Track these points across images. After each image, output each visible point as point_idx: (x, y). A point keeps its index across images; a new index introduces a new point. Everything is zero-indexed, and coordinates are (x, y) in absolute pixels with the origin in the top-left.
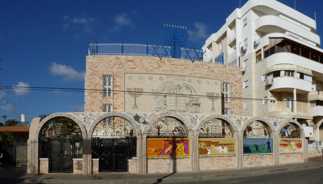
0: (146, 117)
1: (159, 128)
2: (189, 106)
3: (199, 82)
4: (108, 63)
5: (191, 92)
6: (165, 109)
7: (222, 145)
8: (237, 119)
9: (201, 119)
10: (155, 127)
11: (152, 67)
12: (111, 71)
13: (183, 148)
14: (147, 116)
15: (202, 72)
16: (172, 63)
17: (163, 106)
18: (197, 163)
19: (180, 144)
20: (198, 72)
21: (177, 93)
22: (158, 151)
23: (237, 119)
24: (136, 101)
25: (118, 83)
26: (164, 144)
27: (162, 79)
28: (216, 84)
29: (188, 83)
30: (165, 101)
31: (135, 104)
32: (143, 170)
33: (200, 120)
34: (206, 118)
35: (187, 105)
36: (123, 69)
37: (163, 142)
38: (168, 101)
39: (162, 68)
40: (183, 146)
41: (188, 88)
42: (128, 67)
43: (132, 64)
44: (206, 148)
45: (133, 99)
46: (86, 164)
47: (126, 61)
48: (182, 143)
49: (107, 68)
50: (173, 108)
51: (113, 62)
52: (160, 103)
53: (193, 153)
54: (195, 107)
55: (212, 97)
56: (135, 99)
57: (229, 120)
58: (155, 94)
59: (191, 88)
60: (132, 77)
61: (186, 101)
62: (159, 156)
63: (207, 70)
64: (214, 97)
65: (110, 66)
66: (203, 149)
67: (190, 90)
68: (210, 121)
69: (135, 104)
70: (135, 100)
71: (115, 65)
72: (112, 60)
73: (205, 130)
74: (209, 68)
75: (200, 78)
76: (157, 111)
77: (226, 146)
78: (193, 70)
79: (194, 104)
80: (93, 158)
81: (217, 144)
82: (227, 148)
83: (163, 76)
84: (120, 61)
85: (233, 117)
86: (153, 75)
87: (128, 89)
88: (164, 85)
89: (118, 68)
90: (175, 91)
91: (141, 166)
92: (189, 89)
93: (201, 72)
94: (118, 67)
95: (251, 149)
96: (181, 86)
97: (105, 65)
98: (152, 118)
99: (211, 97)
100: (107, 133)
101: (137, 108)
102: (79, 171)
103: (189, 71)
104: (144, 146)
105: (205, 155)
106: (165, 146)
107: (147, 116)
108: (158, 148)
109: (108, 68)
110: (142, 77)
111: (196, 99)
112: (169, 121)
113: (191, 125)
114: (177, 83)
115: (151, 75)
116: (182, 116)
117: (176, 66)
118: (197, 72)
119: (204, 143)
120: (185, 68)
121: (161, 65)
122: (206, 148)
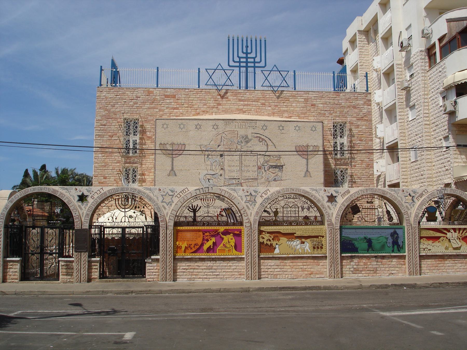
0: (174, 194)
1: (195, 211)
2: (263, 170)
3: (281, 128)
5: (266, 147)
6: (221, 175)
7: (300, 237)
8: (329, 192)
9: (263, 195)
10: (188, 209)
11: (205, 106)
12: (137, 112)
13: (233, 243)
14: (176, 192)
15: (293, 109)
16: (240, 98)
17: (218, 171)
18: (255, 266)
19: (228, 236)
20: (286, 109)
21: (242, 150)
22: (192, 246)
23: (329, 192)
26: (202, 235)
27: (217, 128)
28: (314, 129)
29: (261, 132)
30: (222, 164)
31: (172, 169)
32: (168, 275)
33: (261, 196)
34: (272, 194)
35: (261, 168)
36: (158, 110)
37: (201, 233)
38: (226, 163)
39: (224, 107)
40: (232, 239)
41: (261, 140)
44: (272, 242)
45: (169, 160)
46: (80, 267)
47: (163, 97)
48: (231, 234)
49: (131, 107)
50: (235, 175)
51: (141, 99)
52: (214, 167)
53: (248, 250)
54: (274, 172)
55: (305, 153)
56: (173, 160)
57: (312, 196)
58: (206, 152)
59: (266, 139)
60: (167, 125)
61: (259, 162)
62: (193, 254)
63: (303, 105)
64: (309, 153)
65: (135, 105)
66: (267, 244)
67: (266, 144)
68: (280, 199)
69: (172, 169)
70: (172, 163)
71: (144, 103)
72: (139, 95)
73: (272, 214)
74: (306, 100)
75: (283, 123)
76: (209, 179)
77: (308, 240)
78: (276, 106)
79: (272, 167)
80: (90, 256)
81: (290, 236)
82: (311, 242)
83: (217, 122)
84: (153, 97)
85: (321, 190)
86: (201, 121)
87: (161, 144)
88: (220, 136)
90: (239, 147)
91: (165, 270)
92: (264, 142)
93: (291, 109)
94: (148, 106)
95: (357, 244)
96: (250, 137)
98: (183, 196)
99: (304, 152)
100: (114, 218)
101: (176, 175)
102: (69, 277)
103: (270, 108)
104: (170, 239)
105: (270, 254)
106: (203, 239)
107: (176, 192)
108: (193, 243)
109: (134, 107)
110: (184, 125)
111: (276, 158)
112: (211, 199)
113: (247, 206)
114: (242, 132)
115: (200, 122)
116: (231, 192)
117: (246, 103)
118: (284, 109)
119: (268, 235)
120: (263, 104)
121: (221, 102)
122: (272, 242)
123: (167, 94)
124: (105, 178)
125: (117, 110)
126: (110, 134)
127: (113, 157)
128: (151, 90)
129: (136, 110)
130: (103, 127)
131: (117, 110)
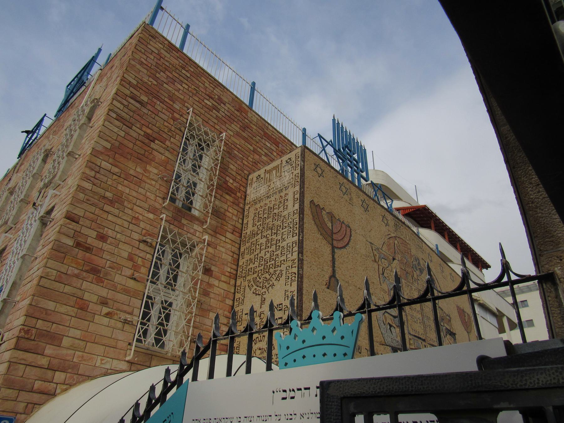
4: (212, 98)
12: (218, 127)
24: (337, 263)
25: (231, 181)
42: (266, 151)
43: (275, 149)
56: (333, 253)
65: (214, 111)
89: (238, 134)
97: (202, 98)
123: (267, 131)
124: (102, 238)
125: (176, 93)
126: (149, 131)
127: (141, 190)
128: (244, 106)
129: (216, 121)
130: (138, 105)
131: (176, 93)
